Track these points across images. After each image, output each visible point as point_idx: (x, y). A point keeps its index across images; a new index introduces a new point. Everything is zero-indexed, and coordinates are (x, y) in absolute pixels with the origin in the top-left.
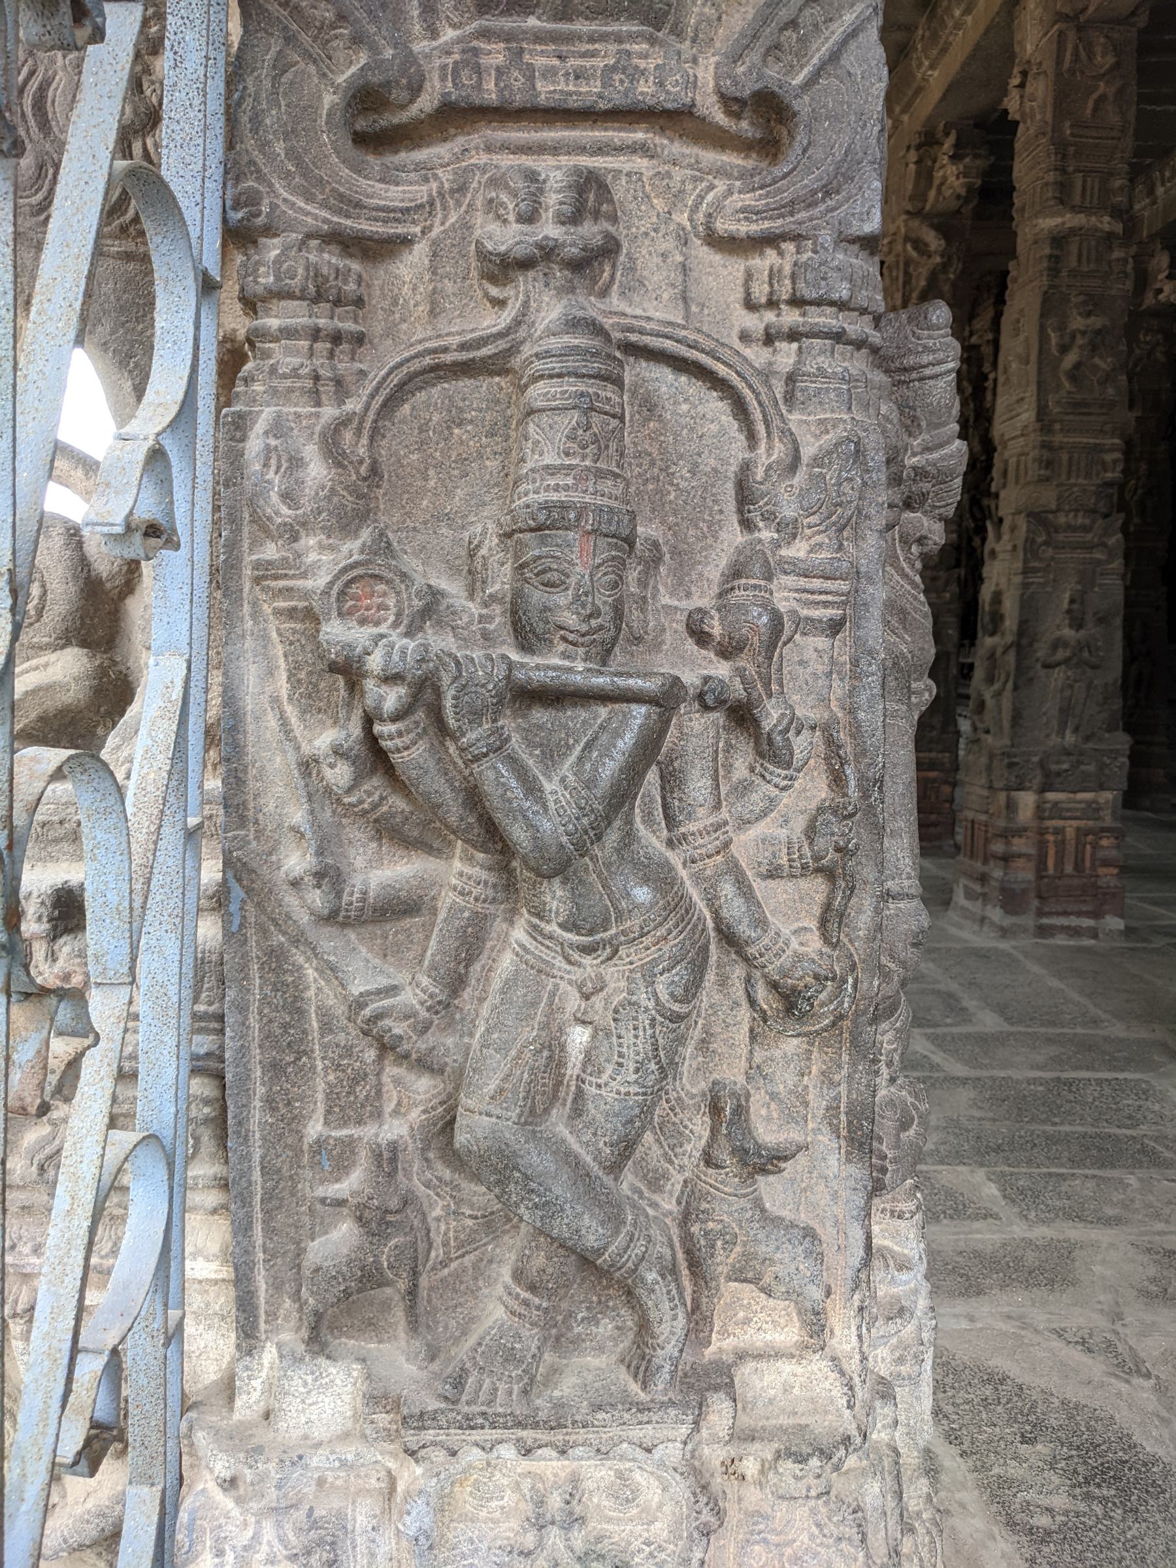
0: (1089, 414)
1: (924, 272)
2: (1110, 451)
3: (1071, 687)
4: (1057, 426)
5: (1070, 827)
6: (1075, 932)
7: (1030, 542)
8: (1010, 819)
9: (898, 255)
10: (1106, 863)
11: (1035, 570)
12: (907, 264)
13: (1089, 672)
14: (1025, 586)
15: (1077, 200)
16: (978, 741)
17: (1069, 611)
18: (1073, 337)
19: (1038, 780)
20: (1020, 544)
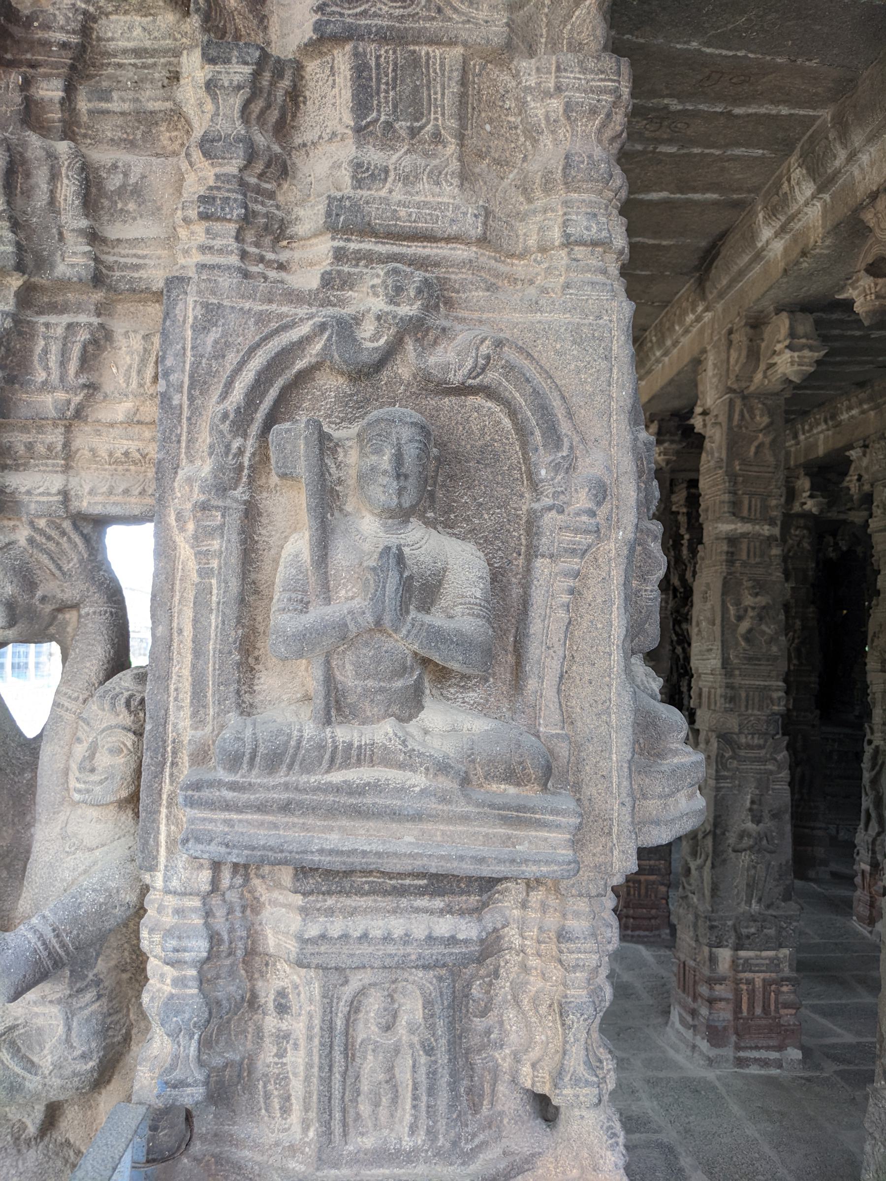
2: (777, 690)
3: (755, 867)
4: (737, 672)
5: (758, 978)
6: (765, 1063)
10: (786, 1006)
13: (768, 856)
14: (718, 789)
15: (745, 513)
16: (686, 897)
17: (750, 810)
18: (746, 611)
20: (713, 758)
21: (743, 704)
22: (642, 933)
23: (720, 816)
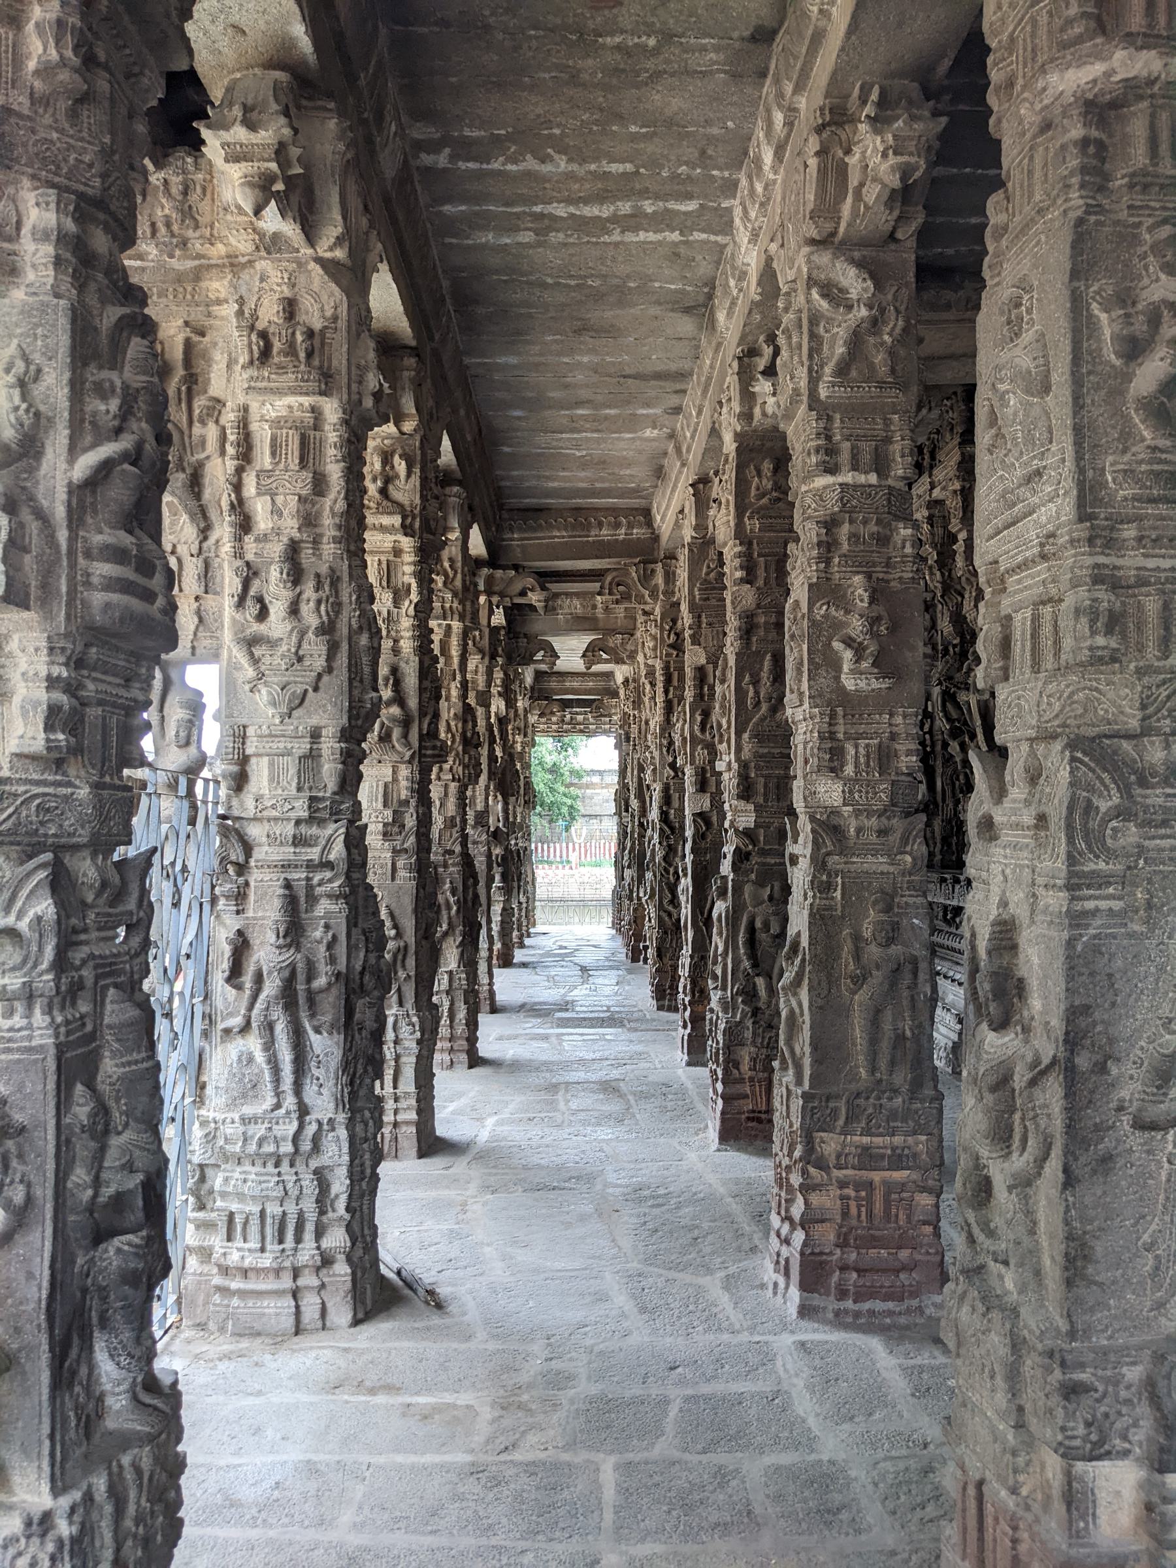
1: (841, 333)
4: (1129, 532)
7: (1080, 812)
8: (1075, 1535)
9: (800, 311)
11: (1100, 881)
12: (814, 320)
14: (1076, 919)
15: (1136, 21)
16: (981, 1268)
18: (1155, 321)
19: (1143, 1431)
20: (1057, 813)
21: (1152, 633)
22: (878, 1305)
23: (1086, 1009)
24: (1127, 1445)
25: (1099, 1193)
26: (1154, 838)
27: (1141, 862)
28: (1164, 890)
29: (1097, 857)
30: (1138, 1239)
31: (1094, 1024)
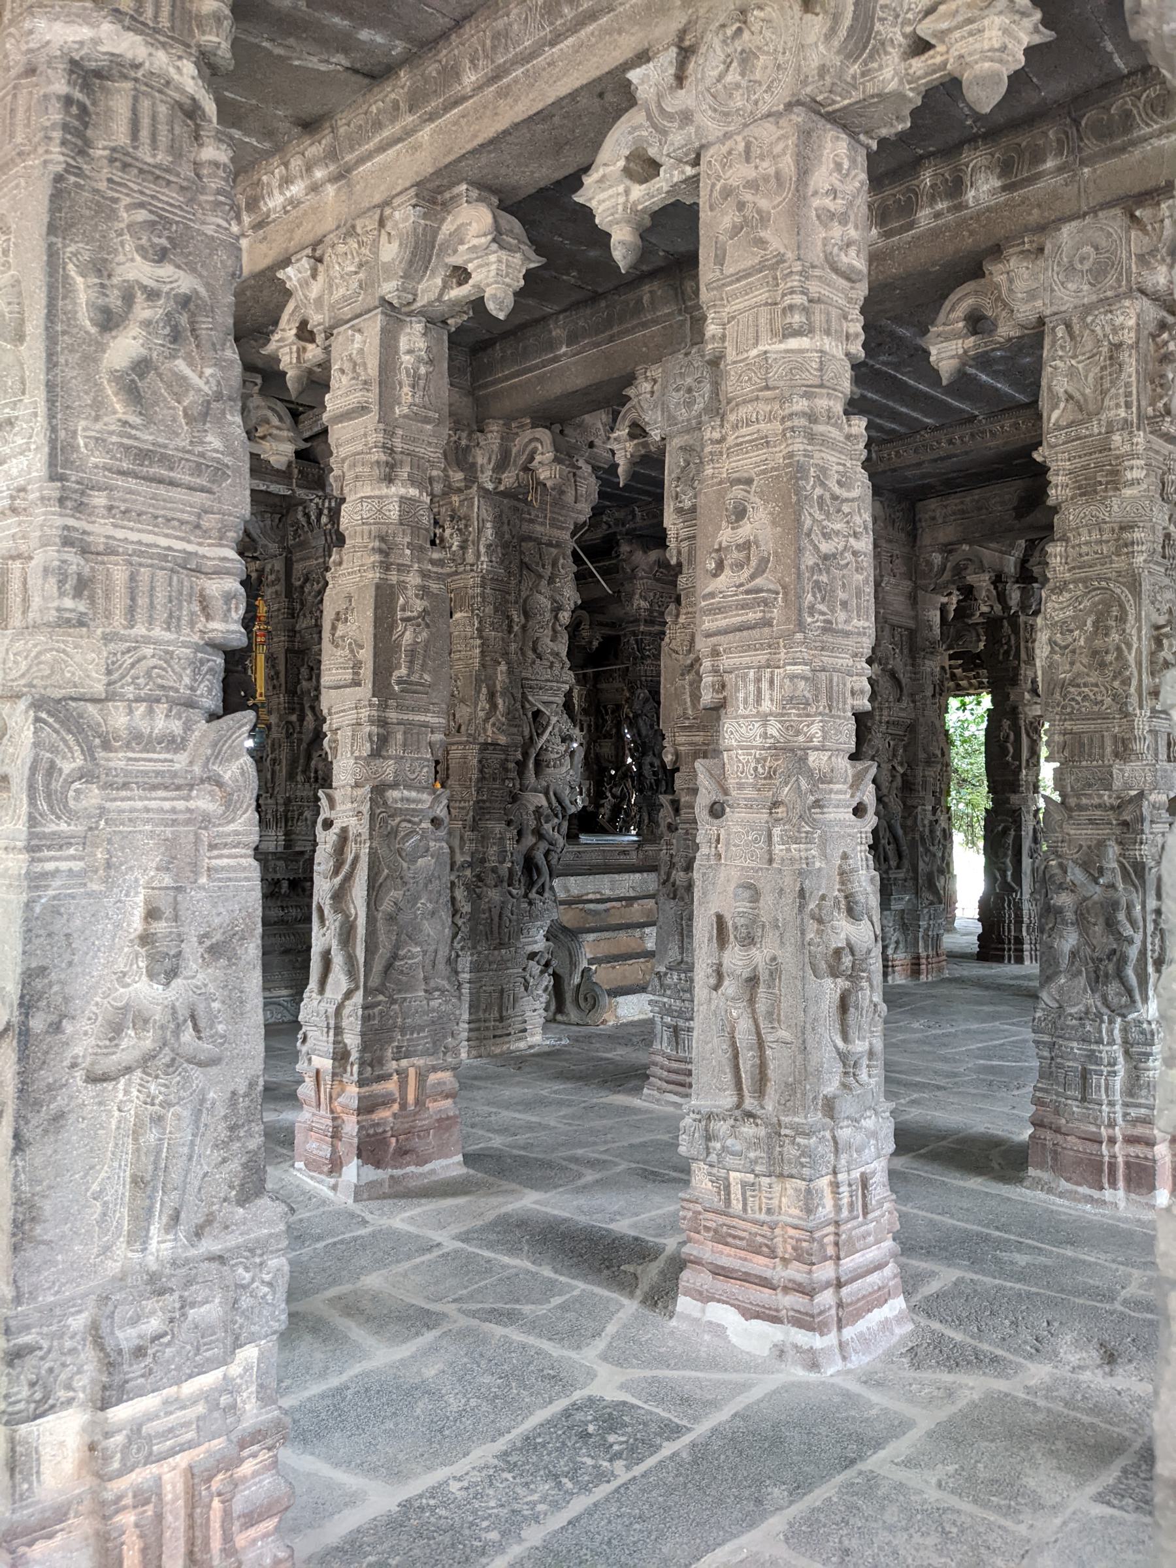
0: (172, 483)
2: (218, 572)
3: (158, 1120)
4: (99, 500)
5: (170, 1476)
7: (43, 775)
8: (16, 1497)
11: (61, 842)
13: (196, 1072)
14: (36, 881)
17: (146, 939)
18: (128, 299)
19: (86, 1373)
21: (119, 602)
23: (42, 971)
24: (71, 1394)
25: (50, 1152)
26: (115, 800)
27: (102, 823)
28: (122, 849)
29: (59, 818)
30: (87, 1190)
31: (51, 985)
